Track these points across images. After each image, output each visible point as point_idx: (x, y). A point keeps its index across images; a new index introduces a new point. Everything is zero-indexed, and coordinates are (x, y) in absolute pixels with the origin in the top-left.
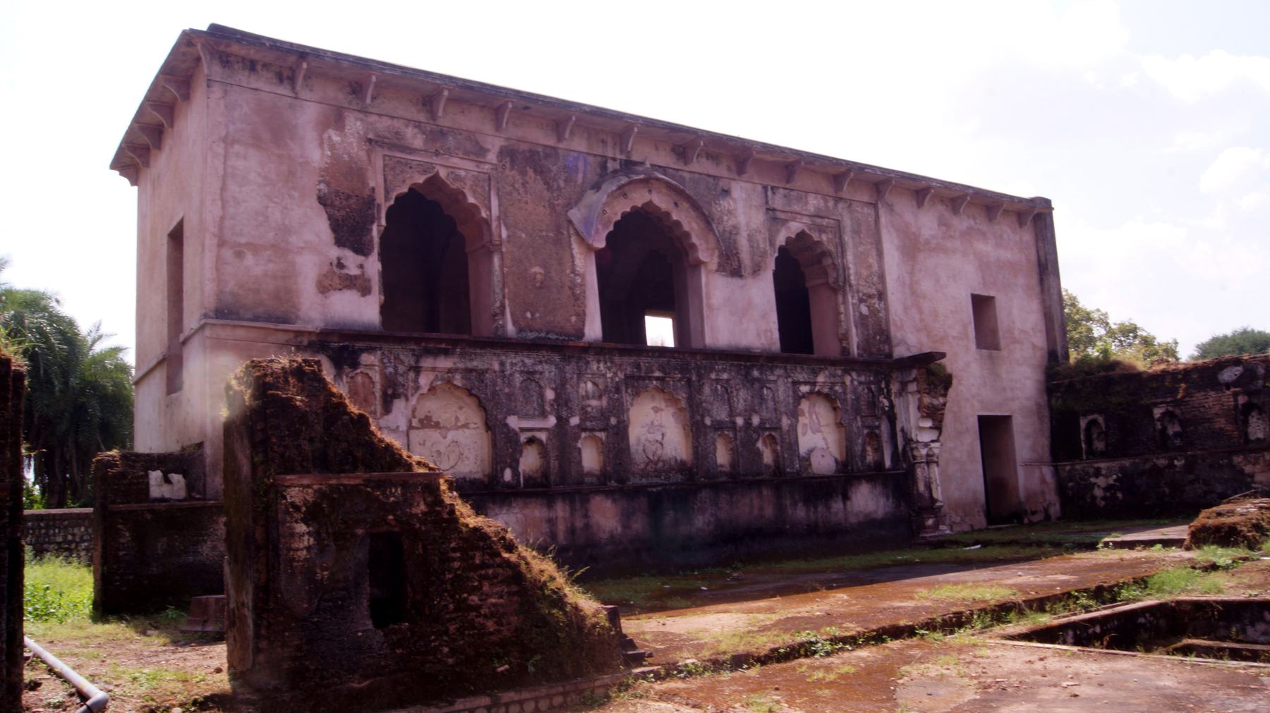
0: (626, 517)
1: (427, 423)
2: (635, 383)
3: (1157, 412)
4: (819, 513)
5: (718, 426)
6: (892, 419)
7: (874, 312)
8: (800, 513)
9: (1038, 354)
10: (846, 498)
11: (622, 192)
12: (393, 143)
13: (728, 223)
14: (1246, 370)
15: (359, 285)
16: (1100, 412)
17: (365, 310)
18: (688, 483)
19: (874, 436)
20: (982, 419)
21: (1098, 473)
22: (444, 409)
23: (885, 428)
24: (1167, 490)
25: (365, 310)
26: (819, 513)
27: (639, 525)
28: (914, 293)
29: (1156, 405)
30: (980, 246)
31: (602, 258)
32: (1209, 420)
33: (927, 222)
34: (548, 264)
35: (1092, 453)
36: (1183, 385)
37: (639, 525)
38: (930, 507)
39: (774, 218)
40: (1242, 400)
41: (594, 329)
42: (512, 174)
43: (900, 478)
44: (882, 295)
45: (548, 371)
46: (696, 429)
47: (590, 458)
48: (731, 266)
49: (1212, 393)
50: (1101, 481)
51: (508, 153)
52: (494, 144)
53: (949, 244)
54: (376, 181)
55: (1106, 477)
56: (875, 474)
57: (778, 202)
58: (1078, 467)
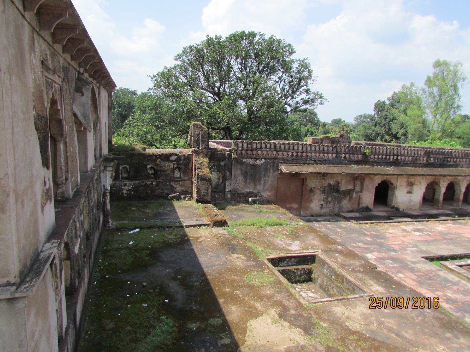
3: (149, 167)
14: (178, 157)
16: (128, 165)
21: (125, 185)
24: (149, 192)
29: (148, 164)
32: (165, 171)
35: (123, 178)
36: (159, 160)
40: (176, 166)
49: (167, 163)
50: (126, 188)
55: (128, 186)
58: (118, 183)
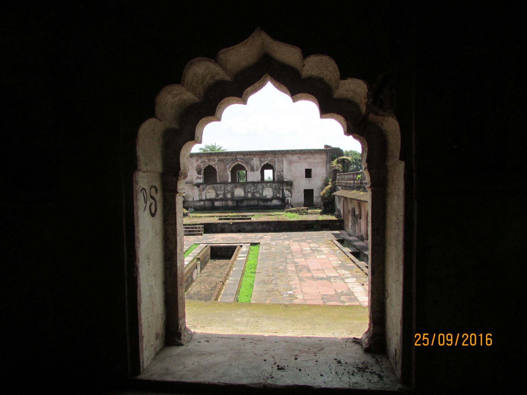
0: (233, 203)
1: (209, 192)
2: (236, 187)
4: (266, 204)
5: (248, 192)
6: (283, 190)
7: (280, 174)
8: (262, 204)
9: (323, 178)
10: (271, 202)
11: (234, 163)
12: (204, 162)
13: (252, 164)
15: (200, 178)
17: (201, 181)
18: (245, 199)
19: (279, 193)
20: (305, 190)
22: (210, 191)
23: (281, 192)
25: (201, 181)
26: (266, 204)
27: (235, 204)
28: (290, 170)
30: (309, 160)
31: (231, 171)
33: (295, 158)
34: (225, 173)
37: (235, 204)
38: (288, 203)
39: (261, 162)
41: (230, 181)
42: (219, 163)
43: (283, 199)
44: (283, 171)
45: (223, 186)
46: (245, 192)
47: (229, 196)
48: (252, 170)
51: (218, 160)
52: (217, 159)
53: (300, 161)
54: (202, 167)
56: (278, 198)
57: (262, 159)
